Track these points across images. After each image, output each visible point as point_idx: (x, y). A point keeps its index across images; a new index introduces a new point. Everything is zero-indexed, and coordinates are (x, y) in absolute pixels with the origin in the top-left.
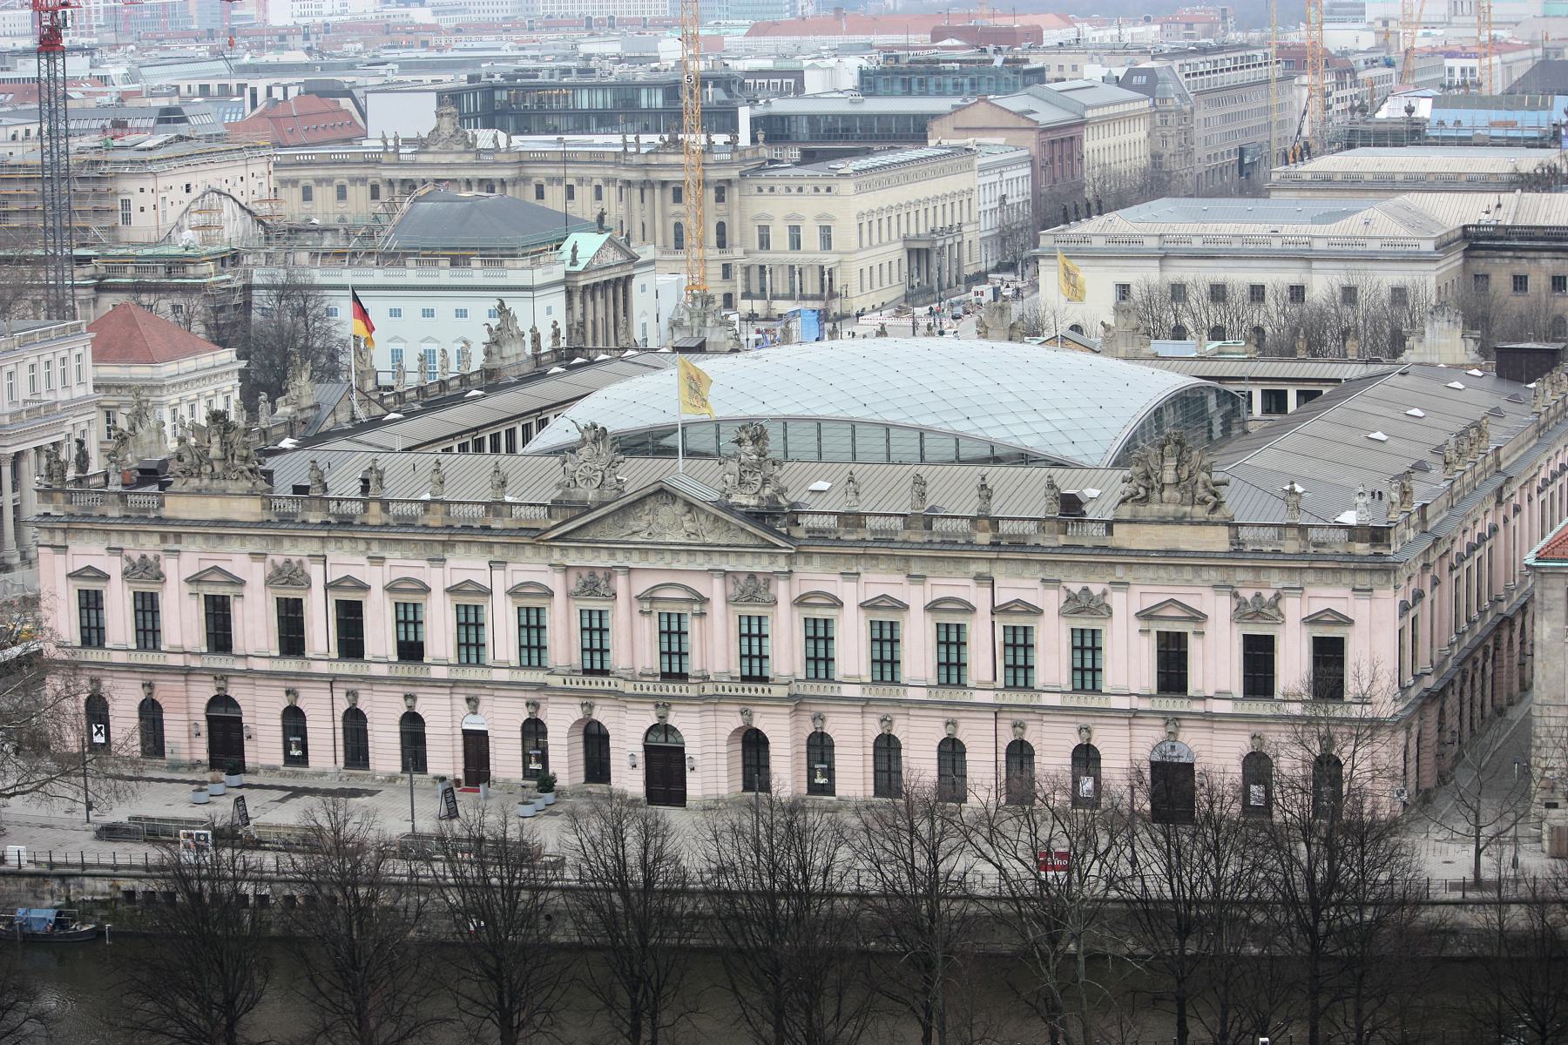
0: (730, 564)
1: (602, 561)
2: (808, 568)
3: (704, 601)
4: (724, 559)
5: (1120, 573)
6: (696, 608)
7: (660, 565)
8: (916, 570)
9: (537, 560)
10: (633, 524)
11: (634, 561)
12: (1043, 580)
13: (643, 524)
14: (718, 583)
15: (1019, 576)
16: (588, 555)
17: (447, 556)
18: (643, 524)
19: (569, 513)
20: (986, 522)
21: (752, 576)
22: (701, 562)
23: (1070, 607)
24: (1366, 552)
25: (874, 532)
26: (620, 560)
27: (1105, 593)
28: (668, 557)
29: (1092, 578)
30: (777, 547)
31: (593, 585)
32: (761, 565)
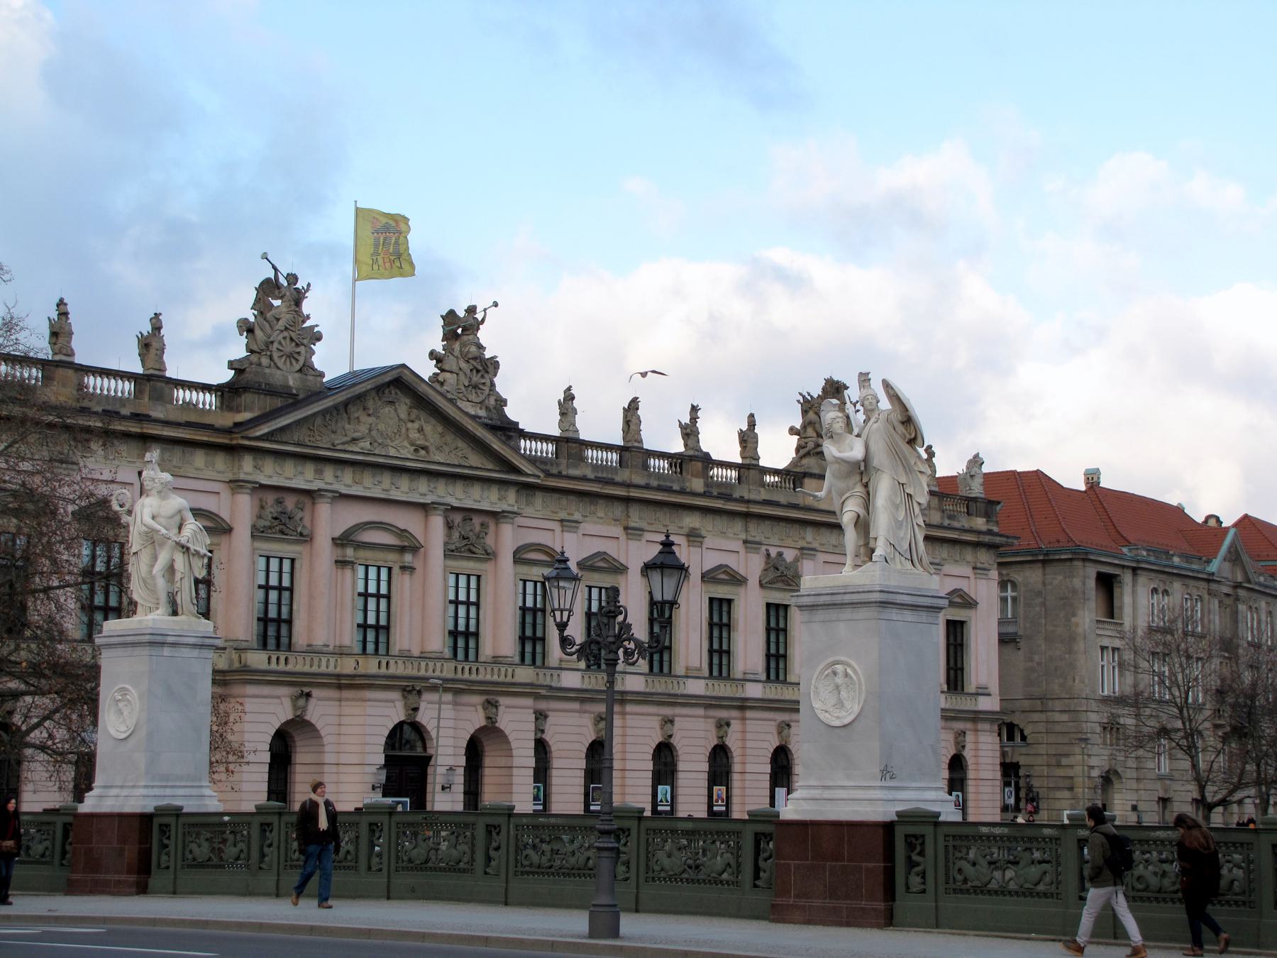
0: (457, 496)
1: (304, 477)
2: (529, 511)
3: (415, 548)
4: (450, 489)
5: (810, 535)
6: (408, 558)
7: (377, 493)
8: (635, 521)
9: (209, 474)
10: (351, 430)
11: (346, 482)
12: (745, 542)
13: (363, 429)
14: (437, 522)
15: (723, 534)
16: (289, 468)
17: (77, 457)
18: (363, 429)
19: (278, 403)
20: (699, 465)
21: (468, 512)
22: (422, 491)
23: (771, 575)
24: (984, 528)
25: (596, 467)
26: (329, 479)
27: (796, 560)
28: (386, 479)
29: (789, 542)
30: (517, 471)
31: (282, 522)
32: (487, 499)
